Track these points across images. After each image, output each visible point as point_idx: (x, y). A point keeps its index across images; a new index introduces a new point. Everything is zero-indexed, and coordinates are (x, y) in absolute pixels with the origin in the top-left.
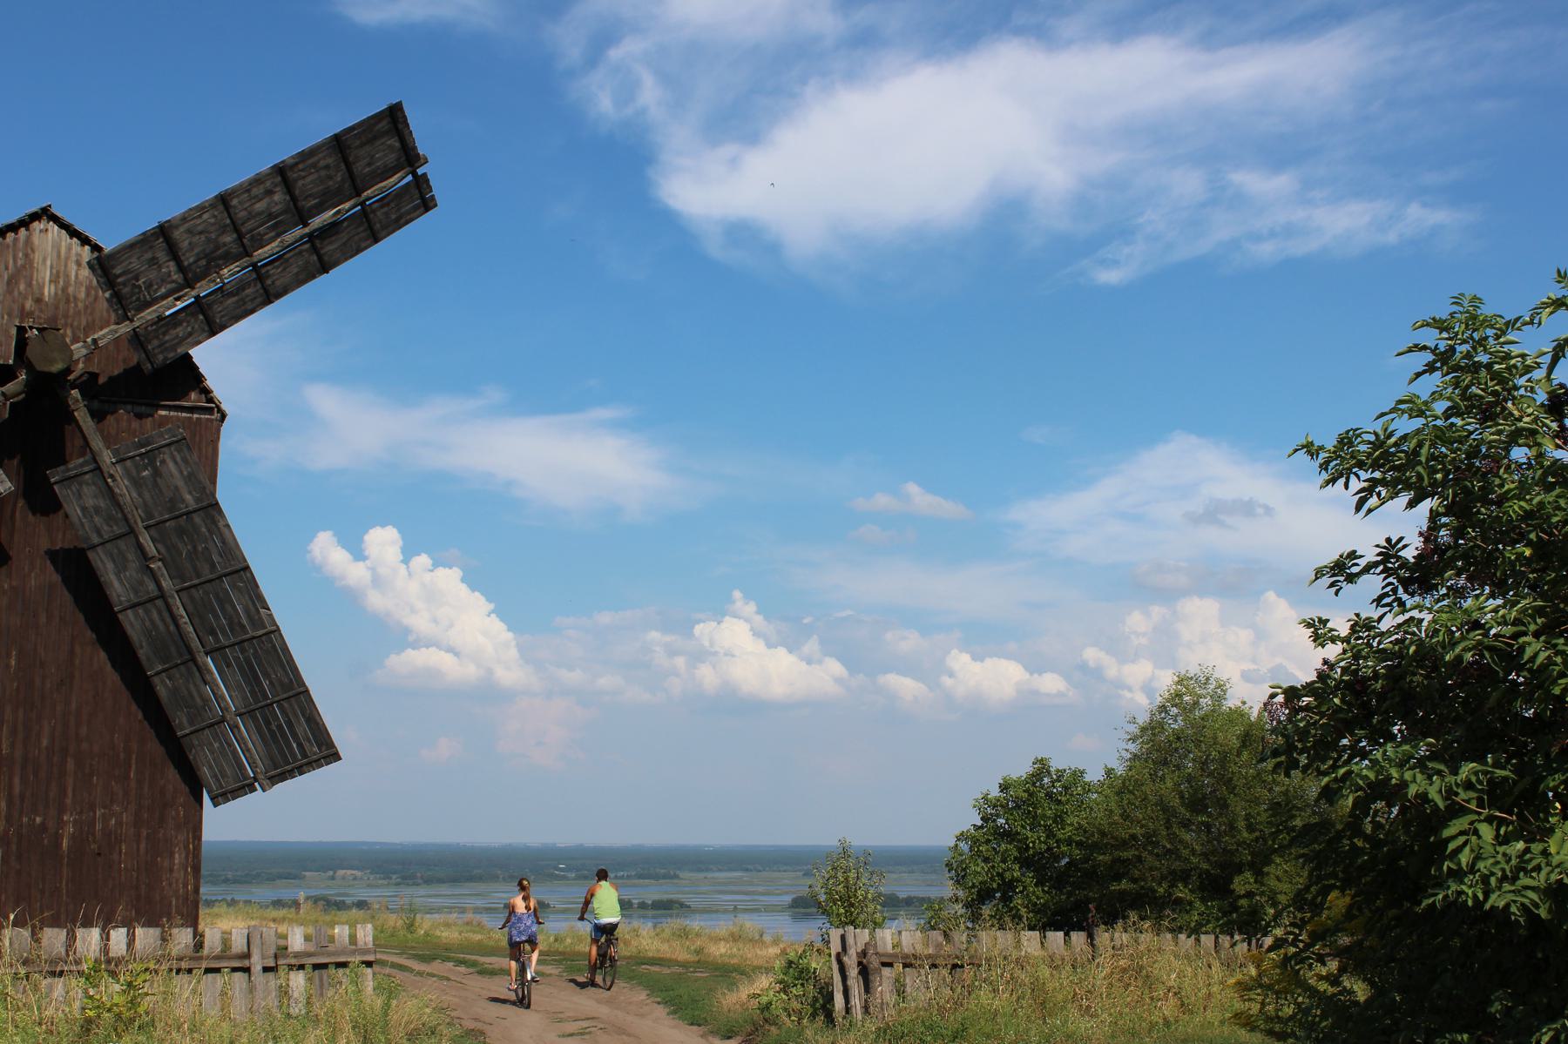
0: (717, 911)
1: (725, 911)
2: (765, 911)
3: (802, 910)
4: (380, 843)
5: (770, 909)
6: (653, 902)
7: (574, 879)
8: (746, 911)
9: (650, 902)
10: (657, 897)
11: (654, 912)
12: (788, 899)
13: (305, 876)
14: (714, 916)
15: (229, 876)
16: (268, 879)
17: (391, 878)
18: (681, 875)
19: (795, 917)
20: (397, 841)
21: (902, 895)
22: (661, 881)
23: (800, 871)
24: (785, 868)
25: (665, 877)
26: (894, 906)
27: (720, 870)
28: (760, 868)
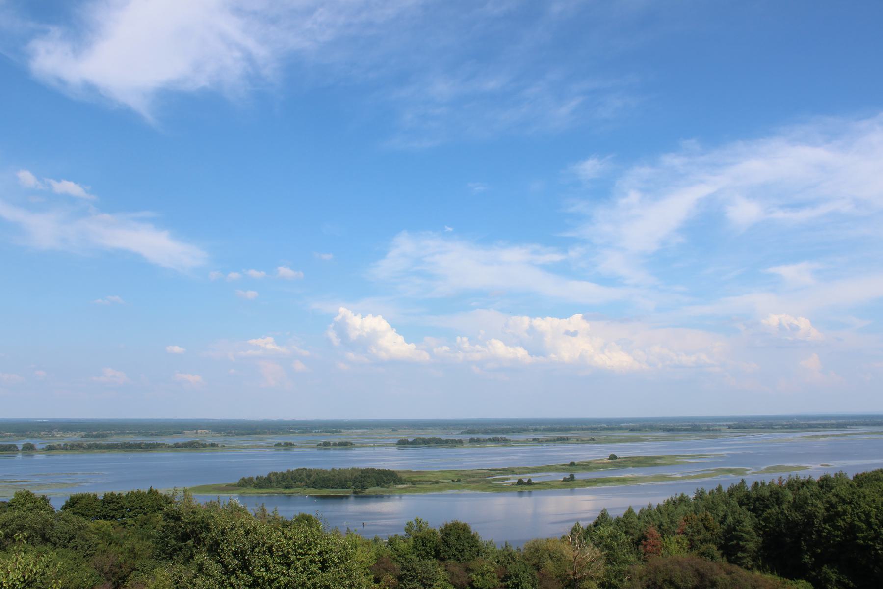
0: (366, 447)
1: (370, 447)
2: (386, 446)
3: (403, 446)
4: (212, 419)
5: (386, 445)
6: (339, 443)
7: (298, 433)
8: (379, 446)
9: (337, 443)
10: (340, 441)
11: (339, 447)
12: (396, 441)
13: (185, 433)
14: (365, 448)
15: (154, 433)
16: (170, 434)
17: (221, 433)
18: (343, 431)
19: (399, 448)
20: (219, 418)
21: (444, 438)
22: (335, 434)
23: (390, 429)
24: (384, 428)
25: (336, 432)
26: (441, 443)
27: (357, 429)
28: (373, 428)
